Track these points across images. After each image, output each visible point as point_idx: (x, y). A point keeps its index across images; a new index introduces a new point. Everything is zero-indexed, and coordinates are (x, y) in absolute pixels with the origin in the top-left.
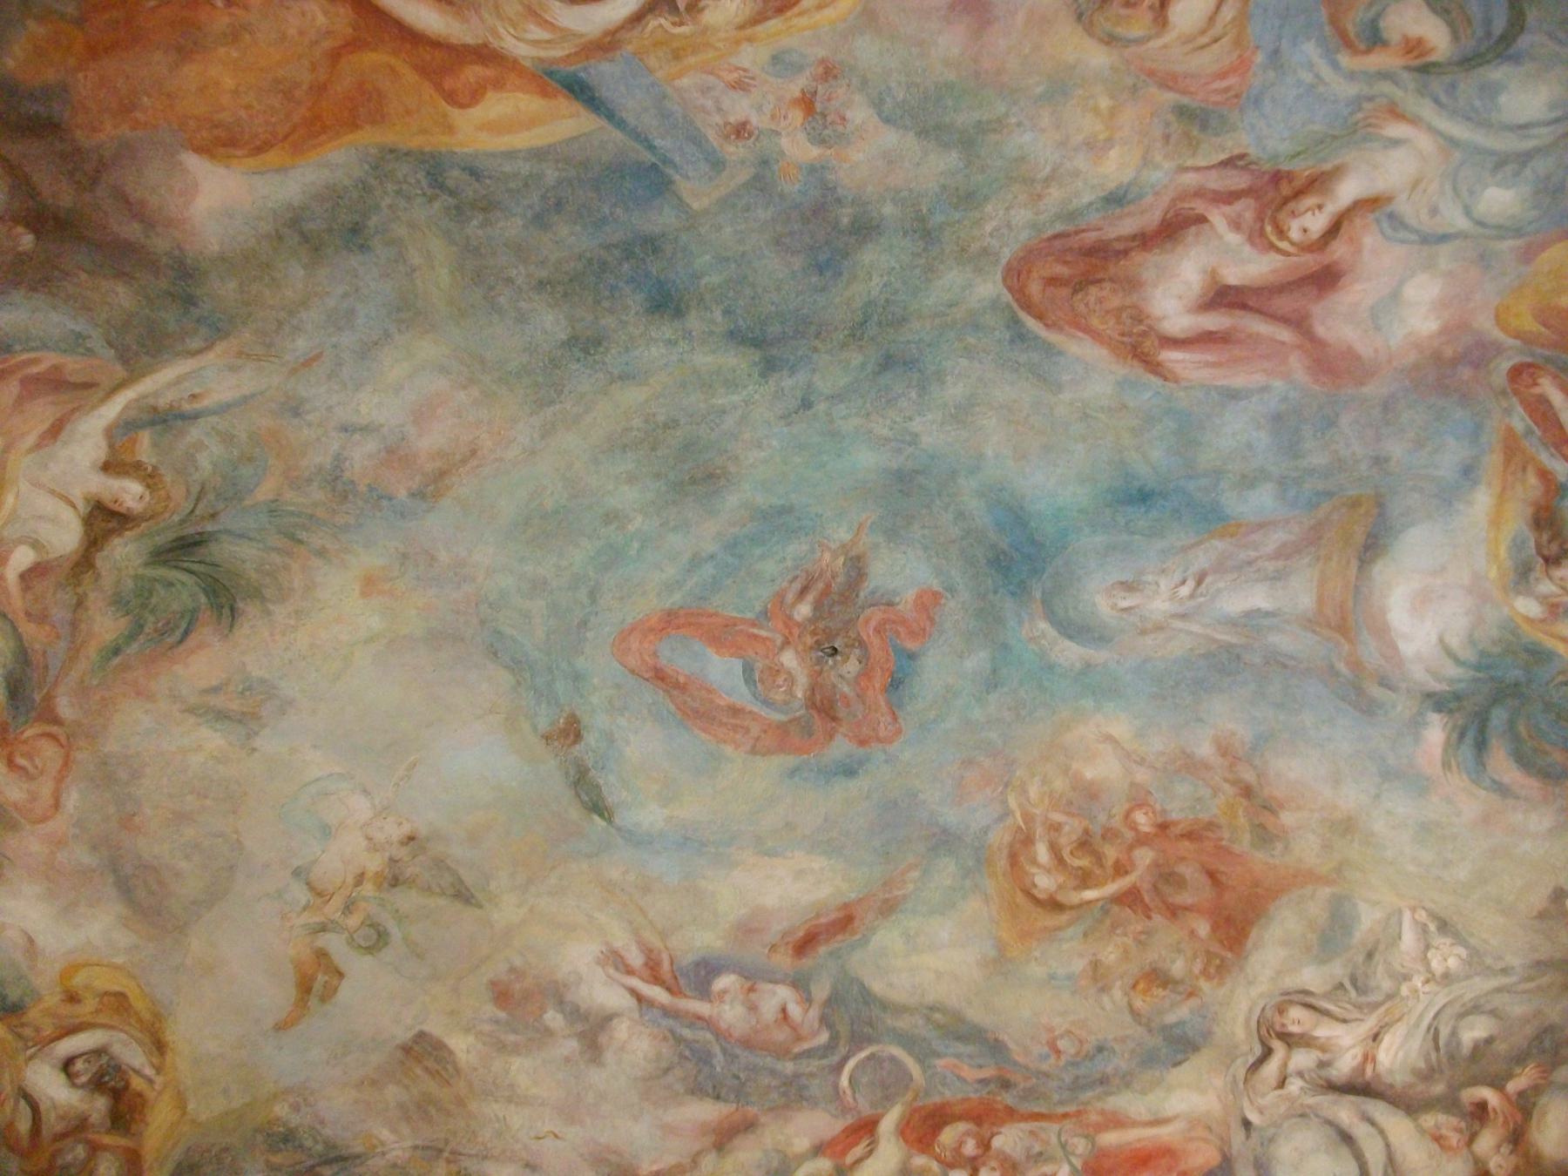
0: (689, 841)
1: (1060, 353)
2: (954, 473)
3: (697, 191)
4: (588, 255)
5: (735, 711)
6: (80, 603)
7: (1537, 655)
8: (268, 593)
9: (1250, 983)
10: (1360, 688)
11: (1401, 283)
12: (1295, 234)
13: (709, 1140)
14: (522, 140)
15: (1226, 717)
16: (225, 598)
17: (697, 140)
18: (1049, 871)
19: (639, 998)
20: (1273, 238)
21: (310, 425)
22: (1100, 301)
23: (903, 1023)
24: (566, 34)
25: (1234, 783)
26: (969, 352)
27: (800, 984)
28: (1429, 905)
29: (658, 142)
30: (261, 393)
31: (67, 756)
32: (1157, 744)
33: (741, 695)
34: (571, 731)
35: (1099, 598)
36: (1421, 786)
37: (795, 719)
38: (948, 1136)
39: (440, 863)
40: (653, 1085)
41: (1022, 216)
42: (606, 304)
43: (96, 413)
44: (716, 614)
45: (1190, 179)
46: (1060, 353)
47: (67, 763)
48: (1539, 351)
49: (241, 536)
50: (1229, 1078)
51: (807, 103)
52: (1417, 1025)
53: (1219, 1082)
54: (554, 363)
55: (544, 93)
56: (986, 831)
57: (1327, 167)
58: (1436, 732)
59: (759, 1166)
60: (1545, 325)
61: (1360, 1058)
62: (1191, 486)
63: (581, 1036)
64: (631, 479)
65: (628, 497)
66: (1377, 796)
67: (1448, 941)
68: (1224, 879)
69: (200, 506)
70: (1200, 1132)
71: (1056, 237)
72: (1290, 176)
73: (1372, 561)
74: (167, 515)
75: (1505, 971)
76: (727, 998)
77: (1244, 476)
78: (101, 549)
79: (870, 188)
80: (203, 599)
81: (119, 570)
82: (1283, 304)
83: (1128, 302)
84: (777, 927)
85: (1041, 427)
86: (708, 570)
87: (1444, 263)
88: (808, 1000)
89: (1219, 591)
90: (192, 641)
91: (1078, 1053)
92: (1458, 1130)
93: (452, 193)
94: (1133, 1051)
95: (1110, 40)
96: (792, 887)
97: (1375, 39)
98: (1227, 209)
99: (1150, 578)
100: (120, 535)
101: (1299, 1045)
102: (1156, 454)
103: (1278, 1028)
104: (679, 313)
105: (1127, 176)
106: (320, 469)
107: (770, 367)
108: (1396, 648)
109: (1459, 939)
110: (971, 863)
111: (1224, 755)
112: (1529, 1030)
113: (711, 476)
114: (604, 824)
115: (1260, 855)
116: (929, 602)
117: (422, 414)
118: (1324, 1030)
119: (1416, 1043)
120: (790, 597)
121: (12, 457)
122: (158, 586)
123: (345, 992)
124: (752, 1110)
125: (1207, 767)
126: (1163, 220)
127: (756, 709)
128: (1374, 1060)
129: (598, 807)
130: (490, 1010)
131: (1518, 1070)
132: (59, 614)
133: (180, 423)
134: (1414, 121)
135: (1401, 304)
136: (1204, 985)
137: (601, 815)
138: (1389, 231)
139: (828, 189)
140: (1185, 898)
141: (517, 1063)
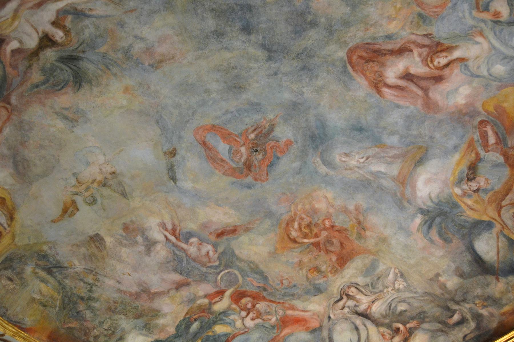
0: (197, 195)
1: (354, 80)
2: (310, 108)
4: (230, 5)
5: (223, 160)
6: (30, 67)
7: (455, 206)
8: (93, 82)
9: (343, 278)
10: (402, 201)
11: (459, 87)
12: (436, 63)
13: (175, 286)
15: (361, 200)
16: (79, 80)
18: (296, 231)
19: (167, 239)
20: (429, 63)
21: (125, 32)
22: (372, 67)
23: (241, 265)
25: (356, 219)
26: (328, 72)
27: (215, 246)
30: (113, 16)
31: (9, 116)
32: (339, 202)
34: (173, 153)
35: (337, 156)
36: (408, 233)
37: (239, 168)
38: (244, 301)
39: (120, 183)
40: (163, 266)
41: (360, 34)
42: (229, 23)
43: (56, 3)
44: (227, 130)
45: (413, 37)
46: (354, 80)
47: (8, 118)
48: (491, 118)
49: (91, 61)
50: (328, 304)
52: (386, 301)
53: (325, 304)
54: (207, 37)
56: (282, 215)
57: (454, 45)
58: (418, 220)
59: (187, 297)
60: (496, 111)
61: (367, 307)
62: (375, 130)
63: (146, 246)
64: (217, 81)
65: (214, 86)
66: (396, 234)
67: (402, 280)
68: (344, 246)
69: (81, 47)
70: (316, 317)
72: (442, 44)
73: (419, 166)
75: (415, 292)
76: (193, 245)
77: (391, 131)
78: (43, 51)
79: (320, 12)
80: (72, 78)
81: (47, 60)
82: (424, 83)
83: (380, 70)
84: (214, 227)
85: (339, 100)
86: (229, 116)
87: (474, 84)
89: (371, 163)
90: (63, 91)
92: (390, 334)
96: (221, 217)
97: (486, 9)
98: (420, 49)
99: (353, 154)
100: (51, 48)
101: (351, 299)
102: (369, 118)
103: (346, 292)
106: (123, 47)
107: (270, 59)
108: (416, 193)
109: (405, 280)
110: (275, 223)
111: (356, 211)
112: (418, 311)
113: (240, 87)
114: (173, 184)
115: (357, 242)
116: (289, 143)
117: (162, 40)
118: (359, 296)
119: (384, 307)
120: (250, 131)
121: (22, 8)
123: (78, 215)
124: (190, 280)
125: (350, 213)
127: (228, 162)
129: (173, 179)
130: (121, 232)
131: (411, 321)
132: (21, 68)
135: (457, 92)
136: (330, 275)
137: (174, 181)
138: (463, 70)
139: (308, 7)
140: (332, 249)
141: (124, 250)
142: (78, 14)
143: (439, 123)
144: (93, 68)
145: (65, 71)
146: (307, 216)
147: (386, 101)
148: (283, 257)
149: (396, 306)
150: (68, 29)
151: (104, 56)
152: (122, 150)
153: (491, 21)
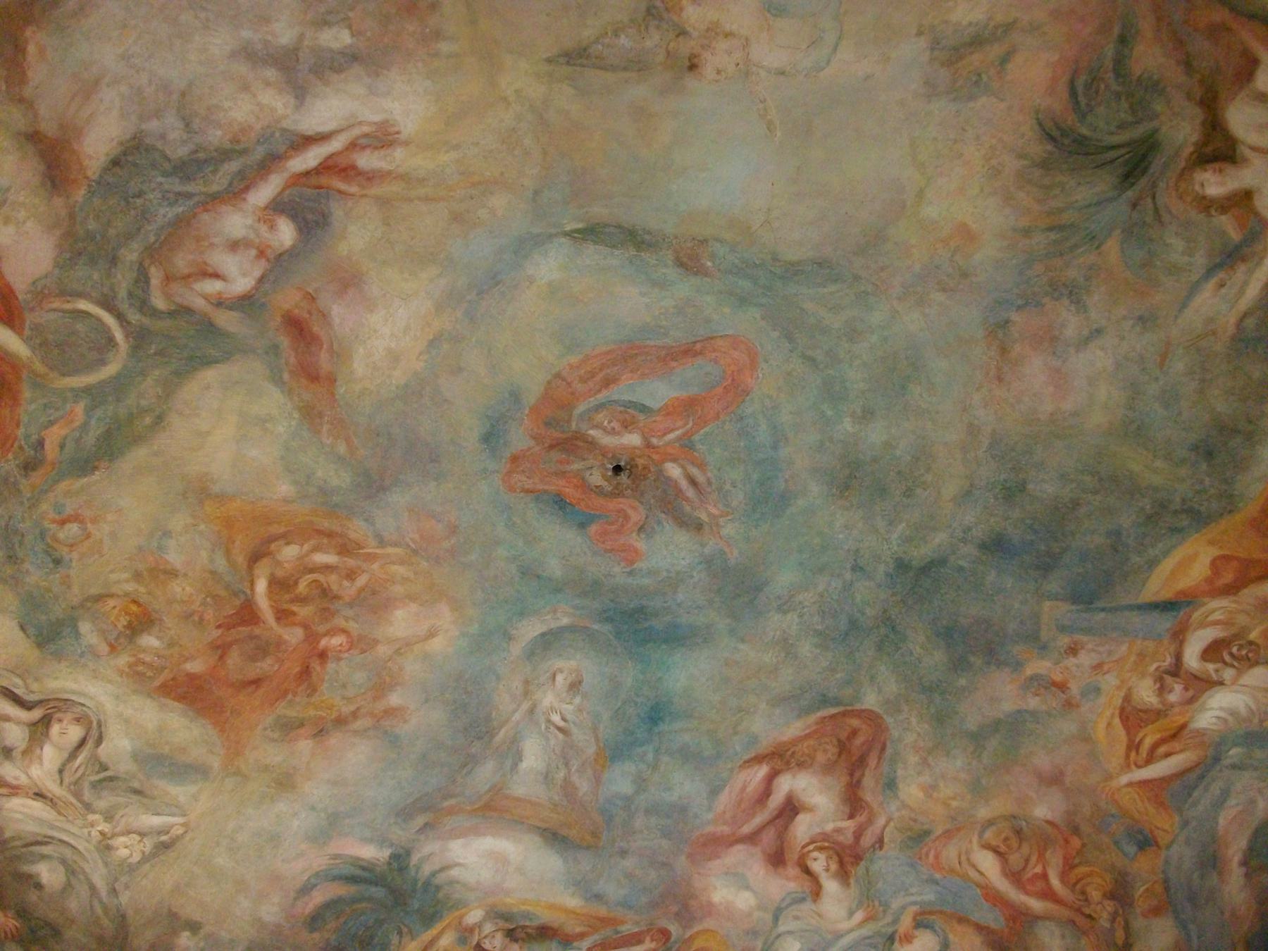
0: (491, 284)
3: (1054, 611)
5: (608, 383)
6: (1188, 65)
8: (1037, 173)
12: (815, 854)
13: (49, 127)
14: (1168, 565)
15: (423, 719)
16: (1065, 145)
17: (1088, 631)
18: (301, 558)
19: (309, 141)
21: (1124, 318)
23: (149, 387)
24: (1203, 625)
27: (246, 303)
28: (187, 838)
29: (1102, 615)
30: (1176, 317)
32: (412, 667)
33: (621, 392)
34: (689, 263)
36: (320, 837)
37: (569, 421)
39: (637, 65)
45: (881, 821)
46: (799, 717)
49: (1099, 203)
51: (1062, 687)
55: (1183, 593)
57: (852, 881)
58: (370, 853)
61: (14, 782)
65: (876, 434)
66: (313, 808)
67: (147, 850)
68: (250, 689)
69: (1151, 206)
71: (883, 749)
73: (542, 835)
74: (1171, 184)
75: (114, 892)
76: (263, 229)
78: (1203, 124)
82: (769, 836)
84: (337, 311)
86: (763, 434)
87: (757, 914)
88: (219, 302)
89: (547, 739)
91: (56, 540)
93: (1176, 512)
94: (49, 590)
95: (991, 822)
99: (578, 700)
100: (1196, 144)
104: (983, 546)
105: (901, 794)
107: (902, 566)
109: (145, 859)
113: (847, 487)
114: (568, 228)
115: (269, 720)
116: (630, 556)
118: (50, 755)
119: (31, 827)
120: (694, 471)
122: (1130, 119)
124: (80, 194)
125: (376, 699)
126: (861, 800)
127: (599, 396)
128: (15, 795)
129: (591, 233)
133: (1218, 260)
134: (861, 925)
135: (736, 889)
136: (123, 660)
137: (577, 231)
139: (1000, 664)
140: (234, 658)
142: (1229, 256)
143: (664, 864)
144: (1079, 197)
145: (1113, 129)
146: (362, 589)
147: (732, 770)
148: (189, 520)
149: (43, 857)
150: (1213, 212)
151: (1095, 241)
152: (770, 126)
153: (895, 932)
